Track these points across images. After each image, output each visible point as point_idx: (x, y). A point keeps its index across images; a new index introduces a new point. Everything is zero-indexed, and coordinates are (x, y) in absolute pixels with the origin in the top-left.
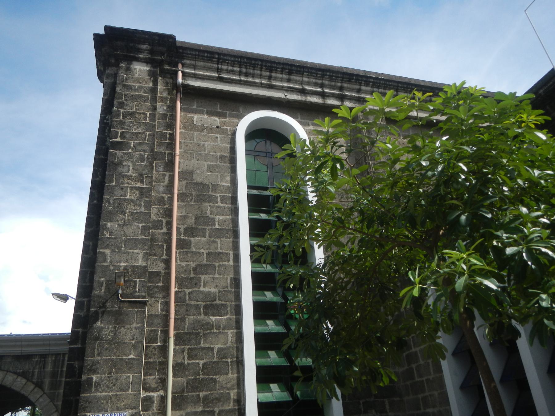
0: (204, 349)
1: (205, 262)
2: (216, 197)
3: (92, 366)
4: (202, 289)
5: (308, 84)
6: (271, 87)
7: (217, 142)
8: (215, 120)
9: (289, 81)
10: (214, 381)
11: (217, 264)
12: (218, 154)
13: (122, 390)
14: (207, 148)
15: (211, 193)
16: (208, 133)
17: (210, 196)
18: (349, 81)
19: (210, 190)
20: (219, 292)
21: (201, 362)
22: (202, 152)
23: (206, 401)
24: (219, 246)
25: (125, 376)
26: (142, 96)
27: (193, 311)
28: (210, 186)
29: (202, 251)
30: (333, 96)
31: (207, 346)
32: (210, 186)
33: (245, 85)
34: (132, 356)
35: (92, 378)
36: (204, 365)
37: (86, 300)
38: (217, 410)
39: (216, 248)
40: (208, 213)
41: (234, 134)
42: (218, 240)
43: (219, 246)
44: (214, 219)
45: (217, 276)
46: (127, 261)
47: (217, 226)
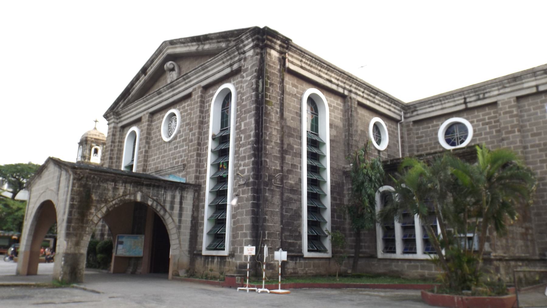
0: (290, 209)
1: (290, 168)
2: (294, 135)
3: (266, 212)
4: (289, 181)
5: (333, 77)
6: (320, 76)
7: (294, 103)
8: (294, 90)
9: (326, 74)
10: (293, 223)
11: (294, 170)
12: (295, 111)
13: (275, 224)
14: (291, 106)
15: (293, 133)
16: (292, 97)
17: (292, 134)
18: (349, 80)
19: (292, 130)
20: (295, 184)
21: (289, 214)
22: (289, 108)
23: (291, 231)
24: (295, 161)
25: (276, 218)
26: (276, 74)
27: (287, 191)
28: (292, 129)
29: (289, 162)
30: (341, 87)
31: (290, 208)
32: (292, 129)
33: (310, 73)
34: (277, 210)
35: (266, 217)
36: (290, 215)
37: (257, 181)
38: (293, 234)
39: (294, 162)
40: (292, 143)
41: (301, 100)
42: (295, 158)
43: (295, 161)
44: (293, 147)
45: (294, 176)
46: (274, 166)
47: (294, 151)
